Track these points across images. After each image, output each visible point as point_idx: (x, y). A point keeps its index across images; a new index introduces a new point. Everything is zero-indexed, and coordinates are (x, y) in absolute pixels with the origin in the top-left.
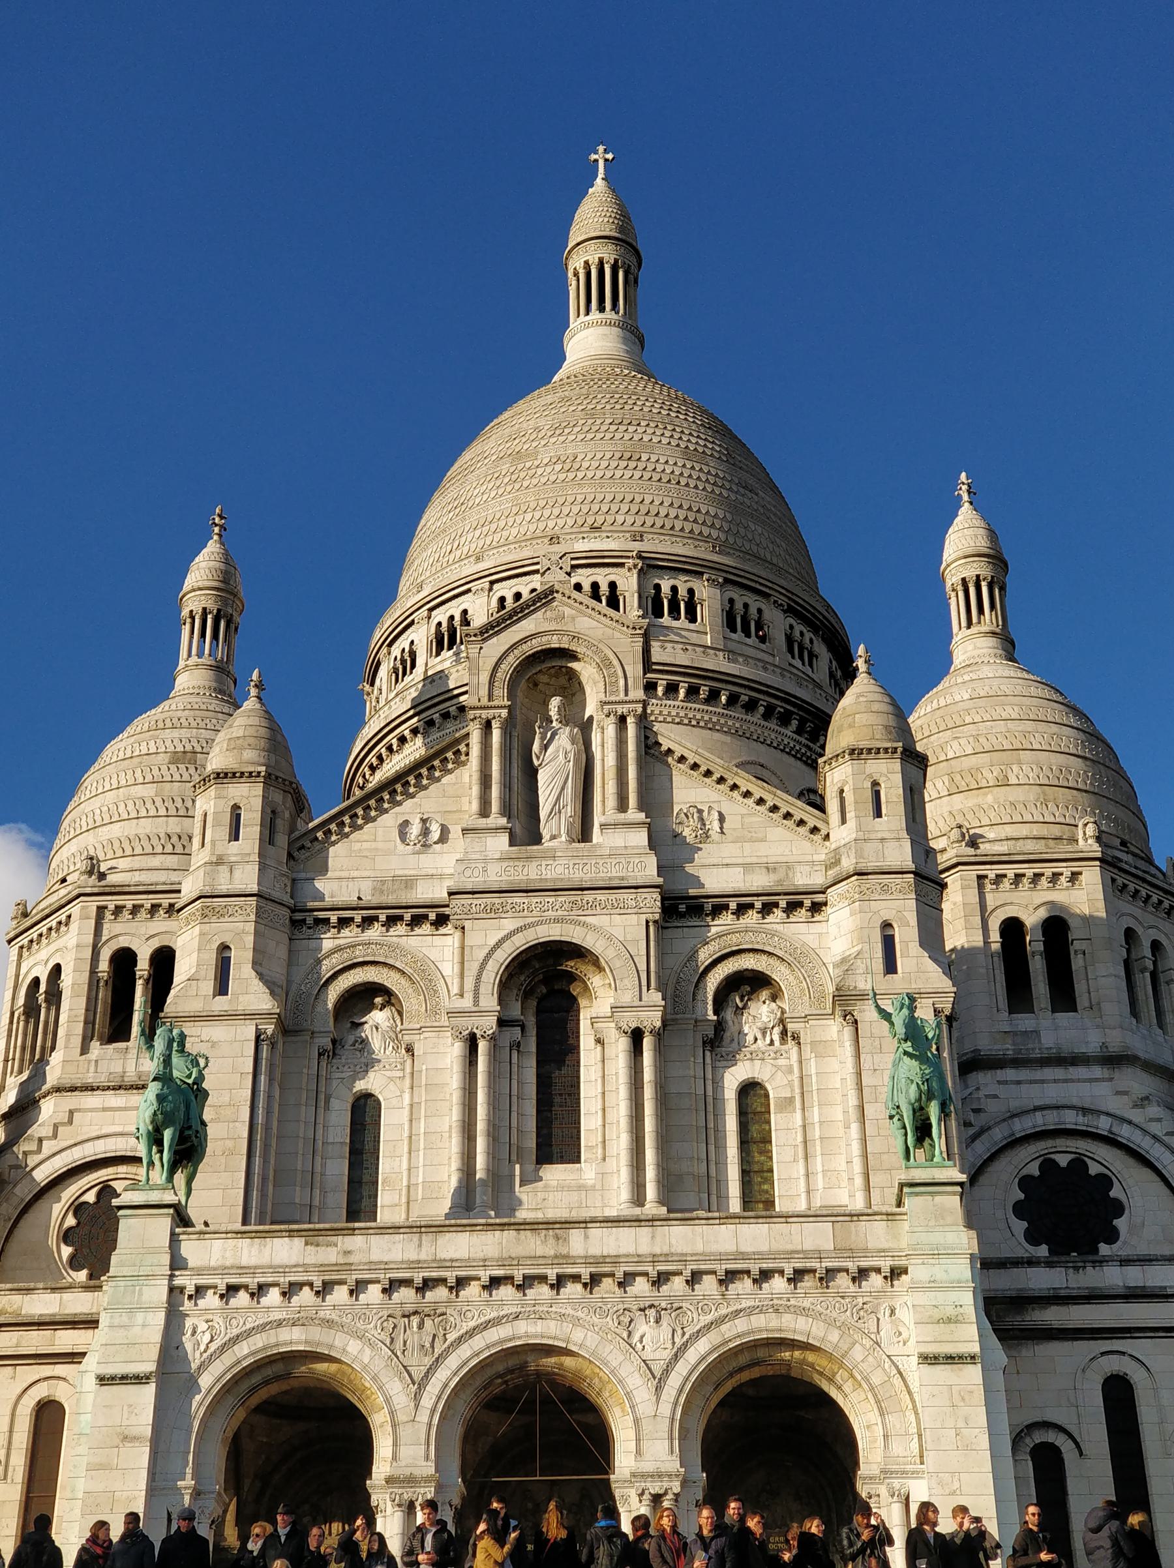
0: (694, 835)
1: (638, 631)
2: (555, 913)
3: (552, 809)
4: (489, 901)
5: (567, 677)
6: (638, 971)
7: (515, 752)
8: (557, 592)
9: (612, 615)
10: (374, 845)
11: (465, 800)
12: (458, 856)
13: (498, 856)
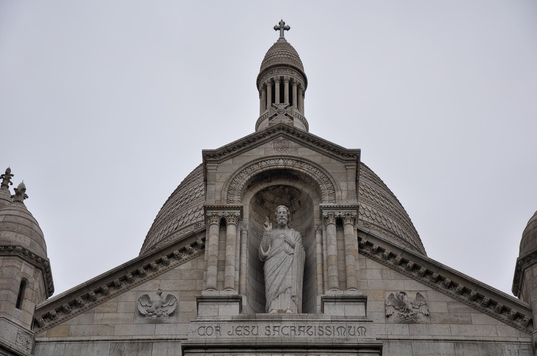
3: (278, 290)
5: (289, 196)
7: (244, 246)
8: (283, 129)
10: (115, 315)
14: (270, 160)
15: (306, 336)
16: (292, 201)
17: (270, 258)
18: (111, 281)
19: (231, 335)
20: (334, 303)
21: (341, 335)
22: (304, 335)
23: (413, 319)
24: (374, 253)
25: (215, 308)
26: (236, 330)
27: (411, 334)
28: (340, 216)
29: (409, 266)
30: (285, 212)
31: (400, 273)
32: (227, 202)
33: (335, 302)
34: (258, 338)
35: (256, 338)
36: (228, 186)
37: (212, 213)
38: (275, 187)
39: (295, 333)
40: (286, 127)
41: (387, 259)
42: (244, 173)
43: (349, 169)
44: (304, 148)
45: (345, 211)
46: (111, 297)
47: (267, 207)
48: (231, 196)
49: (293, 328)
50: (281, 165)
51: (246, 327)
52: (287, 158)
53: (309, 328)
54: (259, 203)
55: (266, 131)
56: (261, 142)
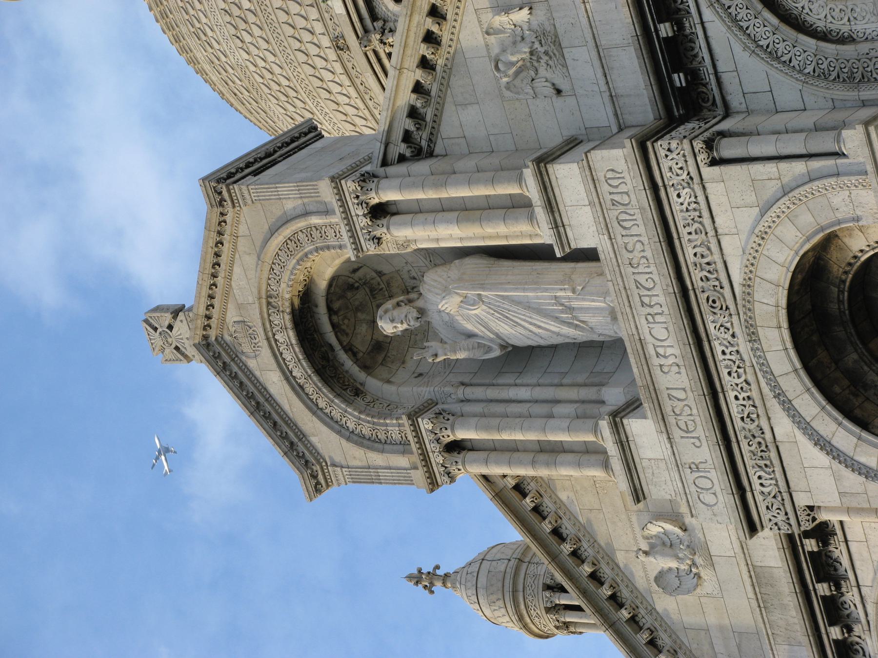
4: (749, 463)
5: (349, 294)
7: (491, 393)
8: (205, 337)
15: (658, 291)
17: (503, 340)
18: (645, 648)
19: (700, 440)
23: (550, 40)
24: (424, 123)
25: (650, 467)
27: (584, 43)
28: (367, 214)
29: (432, 53)
30: (391, 318)
31: (452, 65)
32: (408, 444)
33: (563, 226)
34: (691, 389)
35: (692, 392)
36: (369, 443)
38: (339, 334)
39: (660, 314)
41: (430, 96)
43: (251, 197)
44: (235, 291)
46: (678, 641)
48: (392, 437)
49: (649, 317)
50: (289, 338)
51: (674, 412)
52: (268, 326)
54: (383, 356)
55: (221, 373)
56: (250, 379)
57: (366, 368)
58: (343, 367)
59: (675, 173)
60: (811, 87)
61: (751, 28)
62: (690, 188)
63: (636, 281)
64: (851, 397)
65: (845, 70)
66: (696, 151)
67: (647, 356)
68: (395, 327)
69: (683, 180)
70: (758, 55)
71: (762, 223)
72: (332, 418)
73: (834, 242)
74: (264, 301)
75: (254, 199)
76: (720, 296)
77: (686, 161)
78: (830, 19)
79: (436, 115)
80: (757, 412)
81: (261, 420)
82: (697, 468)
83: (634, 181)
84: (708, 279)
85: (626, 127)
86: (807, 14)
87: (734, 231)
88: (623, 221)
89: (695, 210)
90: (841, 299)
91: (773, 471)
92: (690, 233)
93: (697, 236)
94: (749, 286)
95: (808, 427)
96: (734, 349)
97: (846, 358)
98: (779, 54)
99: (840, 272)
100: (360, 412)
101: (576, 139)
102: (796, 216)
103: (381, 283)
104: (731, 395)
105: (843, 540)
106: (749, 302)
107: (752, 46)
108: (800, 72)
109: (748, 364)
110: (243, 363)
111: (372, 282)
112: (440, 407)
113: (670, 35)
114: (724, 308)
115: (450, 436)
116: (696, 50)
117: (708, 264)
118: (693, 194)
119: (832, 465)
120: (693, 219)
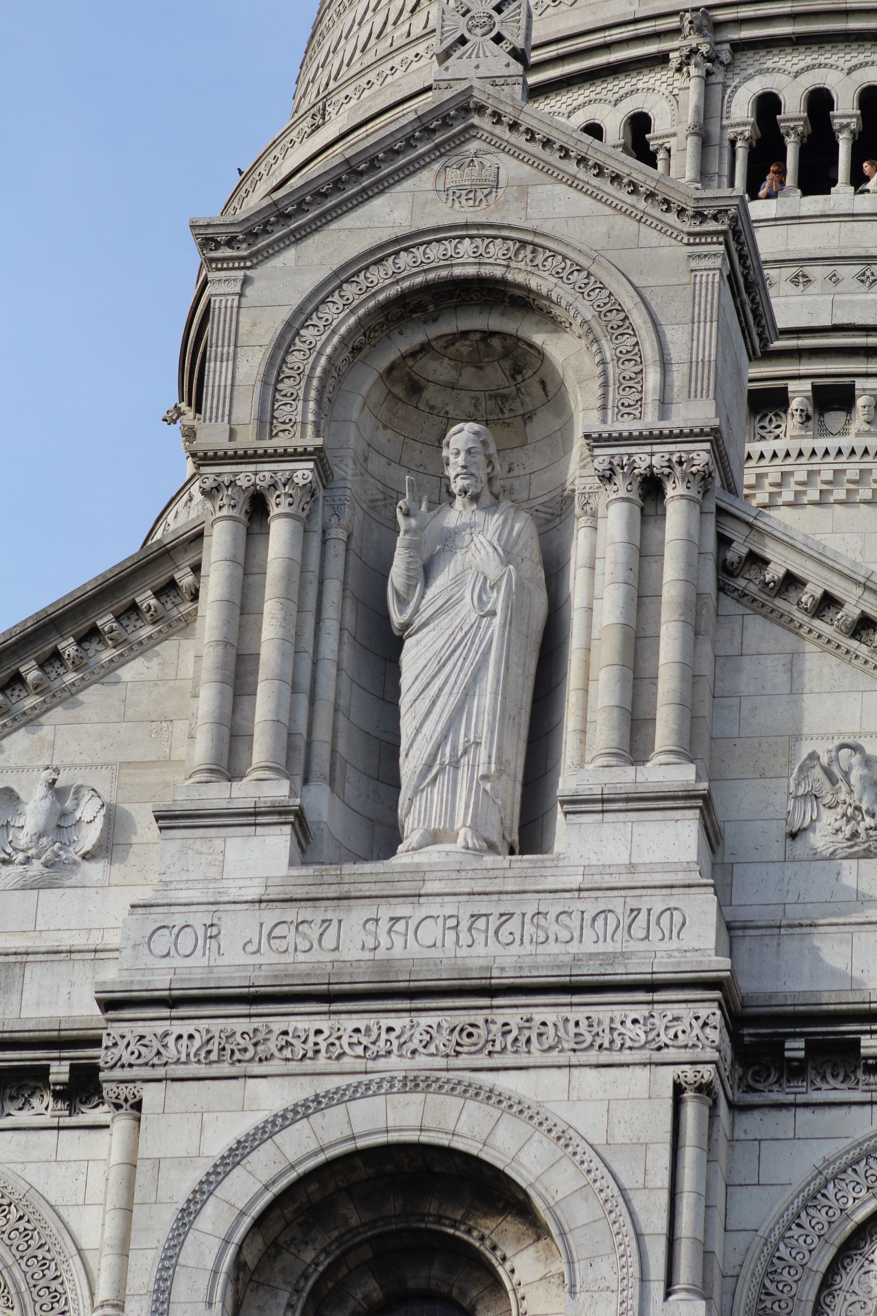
0: (847, 830)
1: (711, 226)
2: (407, 1063)
3: (433, 757)
4: (216, 1026)
5: (507, 364)
6: (639, 1236)
7: (333, 588)
8: (480, 109)
9: (637, 177)
11: (181, 728)
12: (146, 894)
13: (253, 893)
14: (429, 243)
15: (494, 948)
16: (519, 378)
19: (255, 953)
20: (598, 817)
21: (605, 940)
22: (486, 945)
26: (269, 934)
33: (603, 812)
35: (333, 962)
37: (219, 475)
39: (458, 940)
40: (490, 101)
42: (333, 302)
44: (550, 187)
45: (671, 448)
47: (432, 403)
49: (452, 922)
50: (463, 264)
51: (303, 922)
53: (504, 918)
54: (401, 395)
55: (416, 125)
57: (392, 368)
58: (397, 331)
59: (669, 1024)
60: (758, 1252)
61: (855, 1177)
62: (646, 1043)
63: (512, 915)
64: (296, 1205)
65: (776, 1307)
66: (699, 1067)
67: (392, 900)
68: (458, 453)
69: (658, 1035)
70: (814, 1178)
71: (583, 1144)
72: (323, 302)
73: (530, 1232)
74: (529, 238)
75: (699, 273)
76: (478, 1047)
77: (686, 1046)
78: (851, 1298)
79: (782, 615)
80: (293, 1060)
81: (334, 174)
82: (211, 937)
83: (664, 954)
84: (505, 1034)
85: (731, 938)
86: (862, 1266)
87: (574, 1096)
88: (606, 919)
89: (612, 1042)
90: (443, 1221)
91: (199, 1062)
92: (577, 1024)
93: (572, 1035)
94: (489, 1098)
95: (266, 1136)
96: (395, 1047)
97: (352, 1206)
98: (811, 1211)
99: (483, 1230)
100: (330, 358)
101: (718, 843)
102: (587, 1199)
103: (513, 414)
104: (323, 1023)
105: (61, 1124)
106: (465, 1091)
107: (828, 1172)
108: (782, 1238)
109: (371, 1065)
110: (429, 163)
111: (518, 401)
112: (320, 493)
113: (862, 1051)
114: (458, 1049)
115: (277, 507)
116: (833, 1083)
117: (528, 1041)
118: (637, 1045)
119: (204, 1160)
120: (597, 1034)
